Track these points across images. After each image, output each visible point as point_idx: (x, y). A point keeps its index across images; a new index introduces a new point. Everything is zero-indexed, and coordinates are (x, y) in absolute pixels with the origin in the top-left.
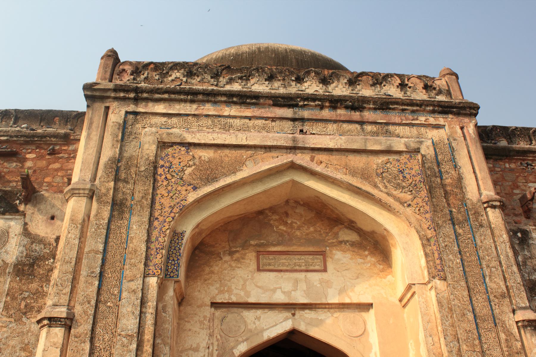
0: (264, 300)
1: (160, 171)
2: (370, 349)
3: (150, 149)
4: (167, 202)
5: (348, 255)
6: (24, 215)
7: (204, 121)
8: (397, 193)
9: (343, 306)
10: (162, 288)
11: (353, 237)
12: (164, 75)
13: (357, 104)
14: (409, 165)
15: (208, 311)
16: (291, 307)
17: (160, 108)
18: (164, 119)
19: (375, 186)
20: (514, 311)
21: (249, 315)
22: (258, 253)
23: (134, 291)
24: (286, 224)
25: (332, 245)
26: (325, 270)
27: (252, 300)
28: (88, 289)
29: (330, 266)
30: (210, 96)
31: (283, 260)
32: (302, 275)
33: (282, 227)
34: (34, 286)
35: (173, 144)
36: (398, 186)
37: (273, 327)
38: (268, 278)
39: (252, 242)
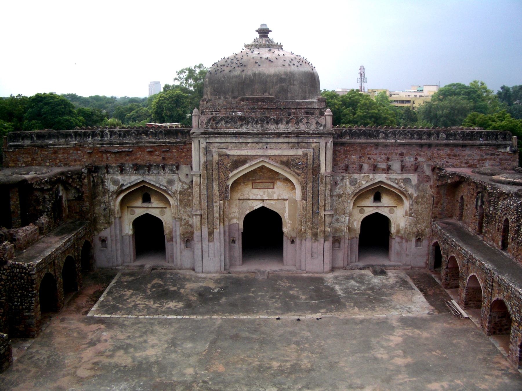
1: (220, 166)
2: (286, 211)
3: (216, 157)
4: (223, 177)
5: (282, 183)
6: (178, 174)
7: (233, 145)
8: (296, 171)
10: (224, 203)
12: (217, 123)
13: (287, 135)
14: (303, 160)
15: (237, 202)
17: (218, 140)
18: (219, 144)
19: (290, 169)
20: (325, 210)
21: (250, 202)
22: (253, 183)
23: (216, 206)
24: (262, 172)
25: (277, 179)
26: (274, 188)
27: (250, 198)
28: (204, 205)
29: (275, 187)
30: (235, 135)
31: (261, 185)
34: (186, 198)
35: (223, 155)
36: (298, 168)
37: (257, 205)
38: (255, 191)
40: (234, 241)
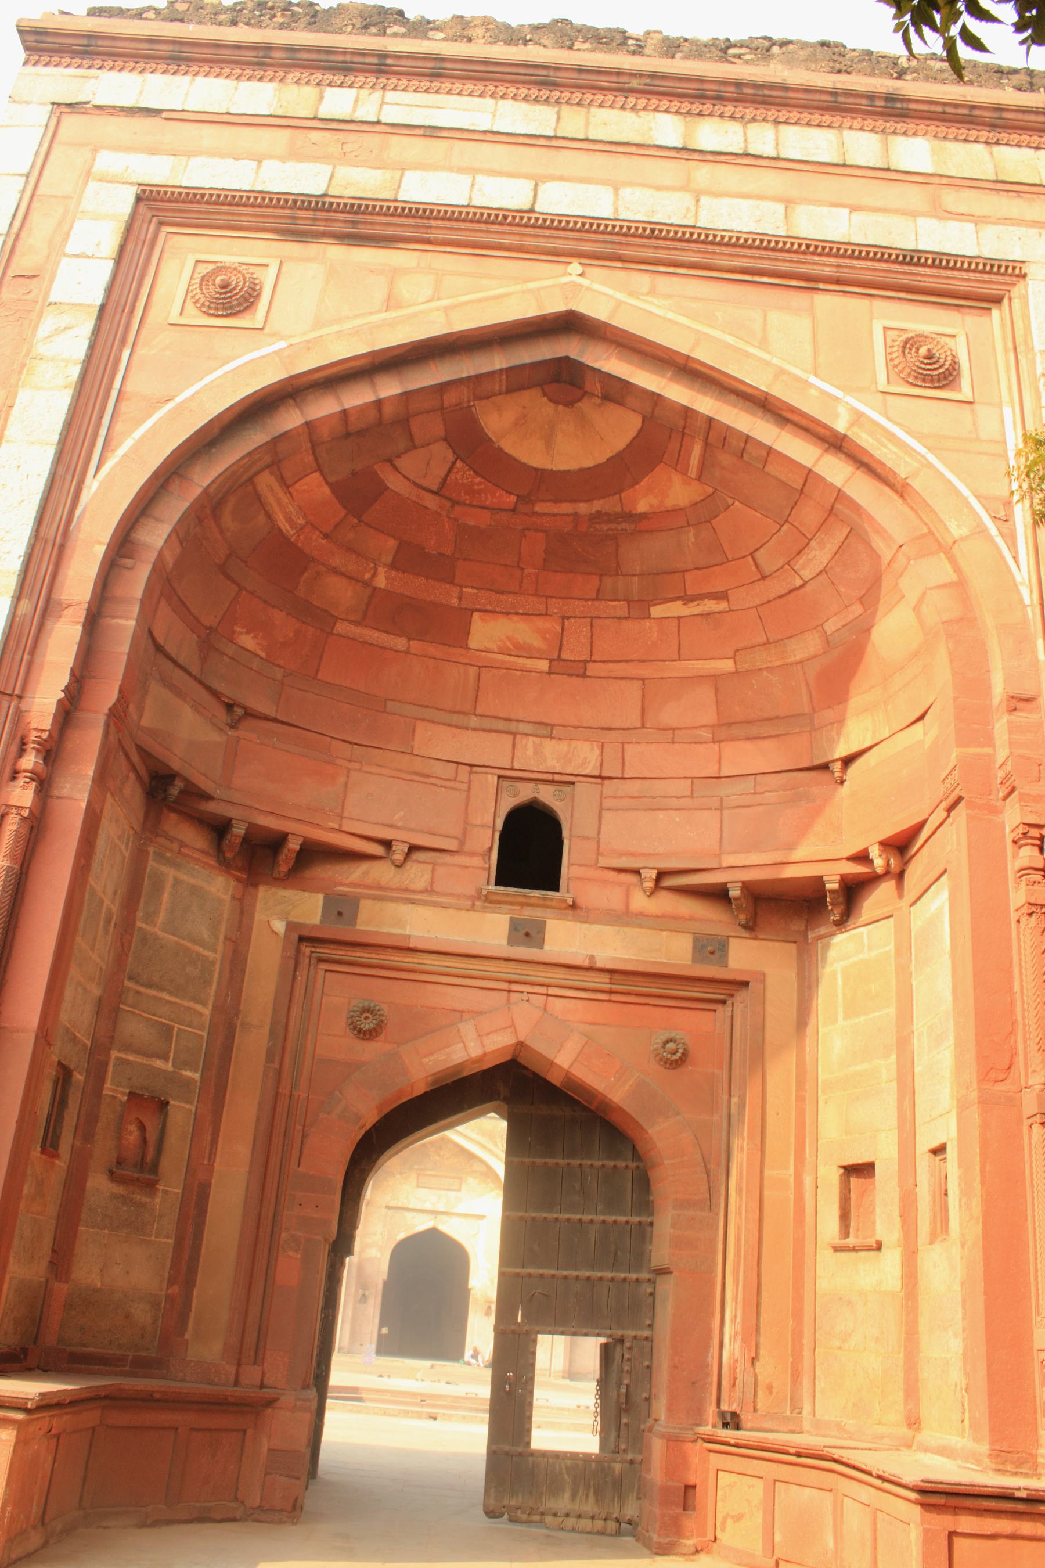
0: (419, 1207)
9: (466, 1215)
11: (482, 1168)
15: (384, 1211)
16: (434, 1213)
21: (408, 1215)
22: (418, 1175)
26: (459, 1190)
27: (411, 1206)
29: (464, 1188)
32: (443, 1192)
33: (437, 1157)
37: (421, 1224)
38: (422, 1192)
39: (416, 1167)
40: (364, 1298)
